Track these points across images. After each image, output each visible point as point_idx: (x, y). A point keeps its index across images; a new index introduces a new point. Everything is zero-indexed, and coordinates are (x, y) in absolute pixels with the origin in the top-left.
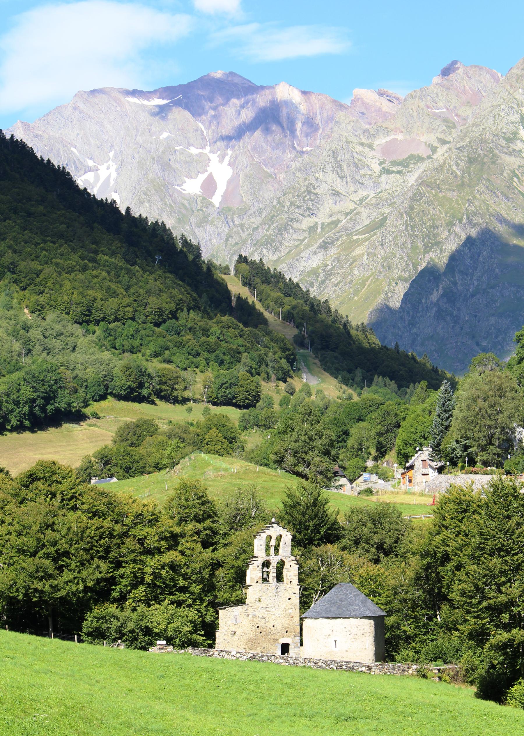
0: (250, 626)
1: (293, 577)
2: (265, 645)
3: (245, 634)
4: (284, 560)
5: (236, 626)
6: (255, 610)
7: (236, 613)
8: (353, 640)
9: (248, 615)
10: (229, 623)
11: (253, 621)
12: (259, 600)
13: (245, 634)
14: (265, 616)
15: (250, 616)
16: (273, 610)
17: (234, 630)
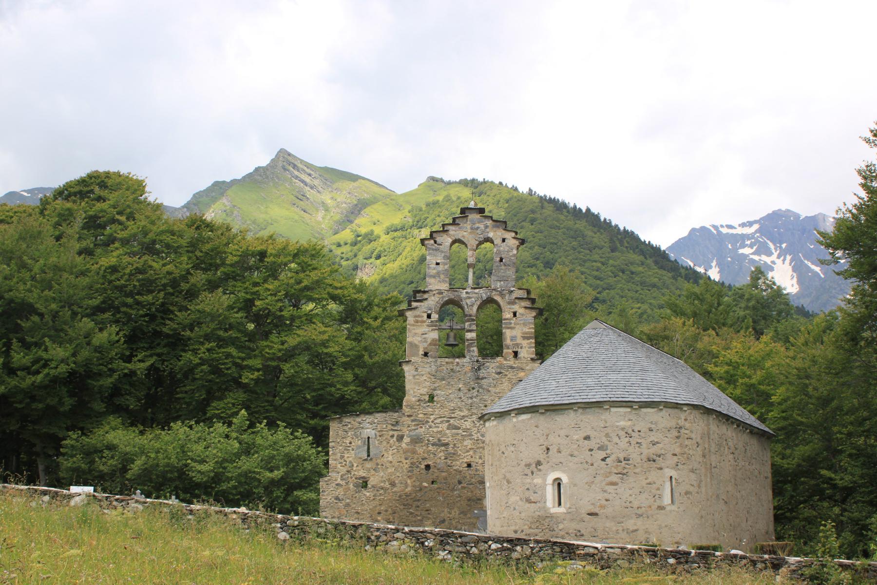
0: (406, 464)
1: (519, 340)
2: (445, 514)
3: (393, 484)
4: (498, 298)
5: (368, 465)
6: (421, 423)
7: (369, 432)
8: (614, 478)
9: (400, 438)
10: (350, 456)
11: (414, 452)
12: (432, 398)
13: (393, 484)
14: (445, 440)
15: (406, 440)
16: (468, 424)
17: (362, 473)
